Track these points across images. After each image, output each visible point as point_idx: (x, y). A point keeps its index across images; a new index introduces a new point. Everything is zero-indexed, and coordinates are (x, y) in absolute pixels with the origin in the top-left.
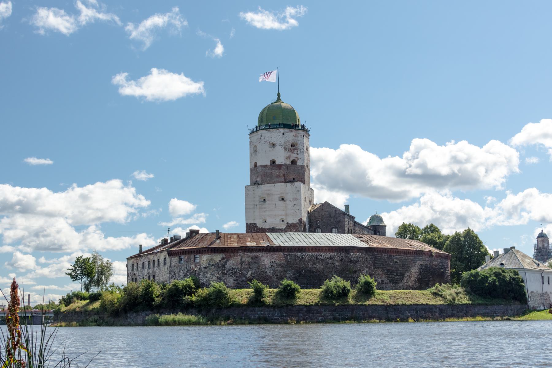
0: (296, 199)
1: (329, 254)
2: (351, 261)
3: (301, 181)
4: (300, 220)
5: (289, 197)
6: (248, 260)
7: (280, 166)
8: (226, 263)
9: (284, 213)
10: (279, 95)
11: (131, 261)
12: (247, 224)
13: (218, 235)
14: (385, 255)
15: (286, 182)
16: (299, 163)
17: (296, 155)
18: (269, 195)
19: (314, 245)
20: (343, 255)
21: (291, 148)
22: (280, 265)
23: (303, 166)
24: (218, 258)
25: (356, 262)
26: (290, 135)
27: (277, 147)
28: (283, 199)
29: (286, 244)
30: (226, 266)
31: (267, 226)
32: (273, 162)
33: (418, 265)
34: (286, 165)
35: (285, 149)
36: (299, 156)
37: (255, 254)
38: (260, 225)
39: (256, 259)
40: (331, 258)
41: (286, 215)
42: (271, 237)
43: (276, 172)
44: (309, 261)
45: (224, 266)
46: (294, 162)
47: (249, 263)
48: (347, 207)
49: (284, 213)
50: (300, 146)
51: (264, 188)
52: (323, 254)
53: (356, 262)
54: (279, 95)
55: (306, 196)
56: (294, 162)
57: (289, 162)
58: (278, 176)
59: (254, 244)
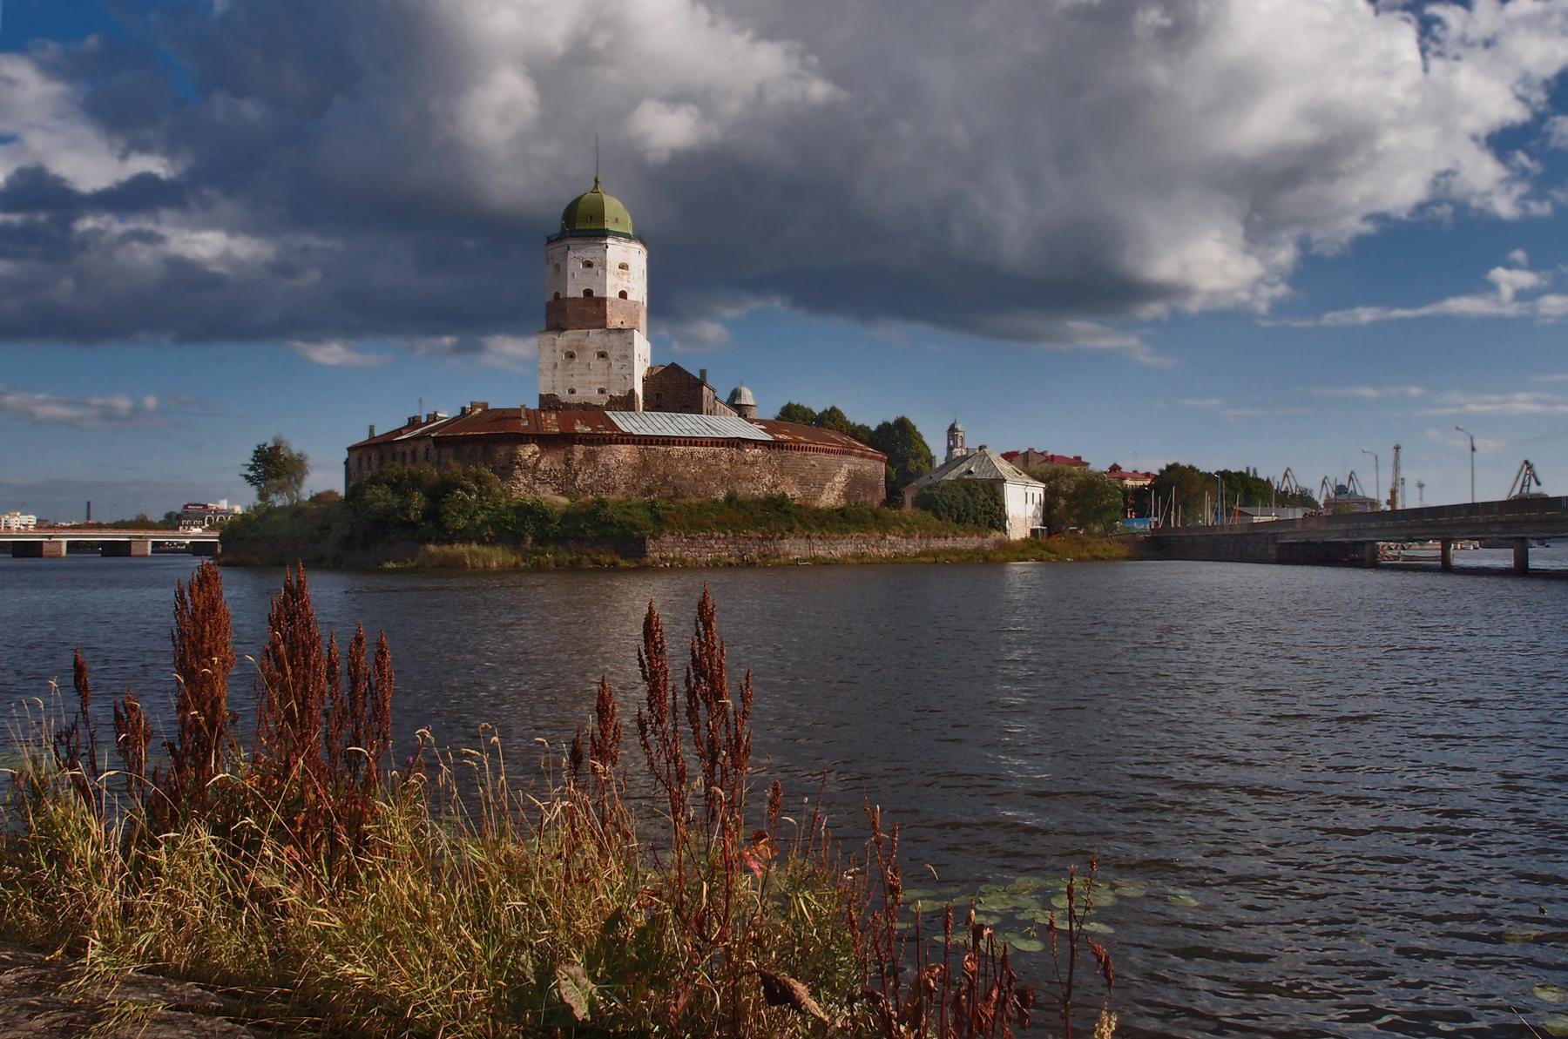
0: (626, 356)
2: (745, 463)
4: (632, 392)
5: (611, 354)
8: (538, 460)
9: (603, 379)
11: (356, 454)
18: (581, 349)
19: (687, 434)
24: (528, 451)
25: (753, 464)
28: (602, 355)
29: (643, 432)
30: (541, 466)
31: (575, 399)
32: (588, 293)
33: (844, 471)
38: (563, 395)
40: (714, 456)
42: (614, 419)
44: (678, 461)
45: (536, 464)
46: (623, 295)
47: (580, 462)
48: (703, 373)
49: (603, 379)
51: (570, 335)
52: (702, 449)
53: (753, 464)
56: (623, 295)
59: (588, 429)
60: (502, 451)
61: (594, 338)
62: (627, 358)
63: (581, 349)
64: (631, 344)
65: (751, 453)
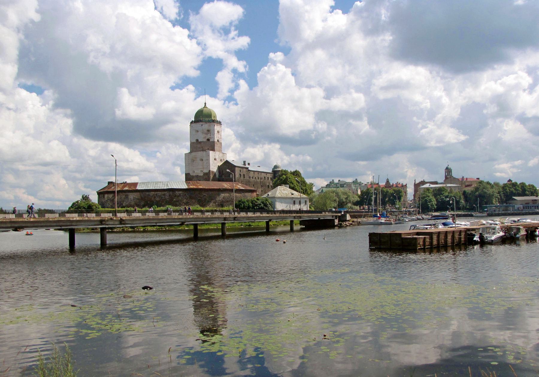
1: (163, 193)
3: (213, 150)
5: (204, 159)
6: (124, 196)
7: (200, 142)
10: (205, 104)
12: (186, 174)
13: (125, 184)
14: (197, 192)
15: (203, 151)
16: (211, 140)
17: (209, 136)
18: (196, 158)
20: (171, 193)
21: (206, 132)
22: (138, 199)
23: (214, 142)
25: (178, 196)
26: (206, 126)
27: (199, 132)
32: (197, 140)
34: (203, 142)
35: (203, 133)
36: (212, 136)
37: (127, 193)
38: (192, 174)
39: (127, 197)
40: (164, 195)
41: (203, 168)
43: (199, 146)
46: (208, 140)
50: (212, 131)
52: (160, 193)
53: (178, 196)
54: (205, 104)
55: (217, 157)
56: (208, 140)
57: (205, 140)
58: (199, 148)
60: (106, 196)
61: (200, 154)
62: (208, 160)
63: (196, 158)
64: (209, 155)
65: (177, 193)
